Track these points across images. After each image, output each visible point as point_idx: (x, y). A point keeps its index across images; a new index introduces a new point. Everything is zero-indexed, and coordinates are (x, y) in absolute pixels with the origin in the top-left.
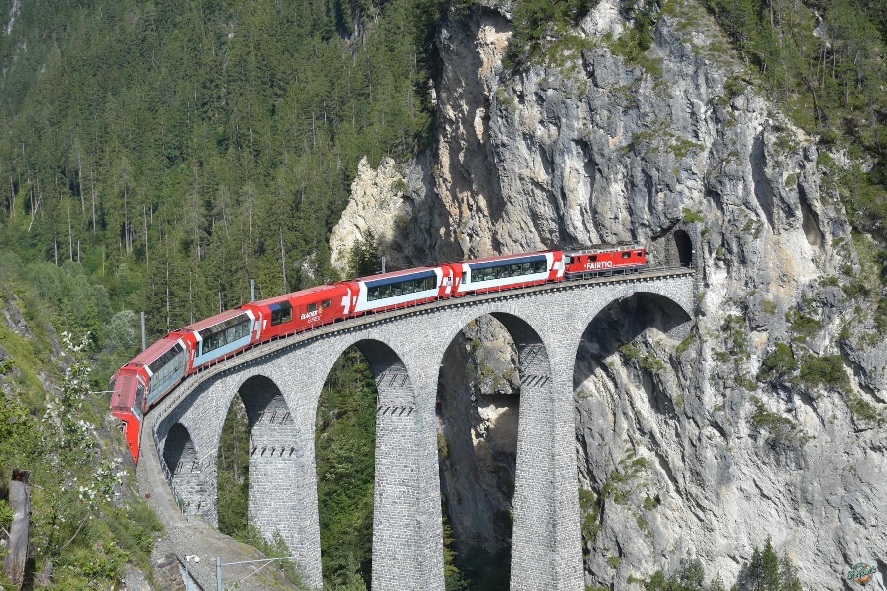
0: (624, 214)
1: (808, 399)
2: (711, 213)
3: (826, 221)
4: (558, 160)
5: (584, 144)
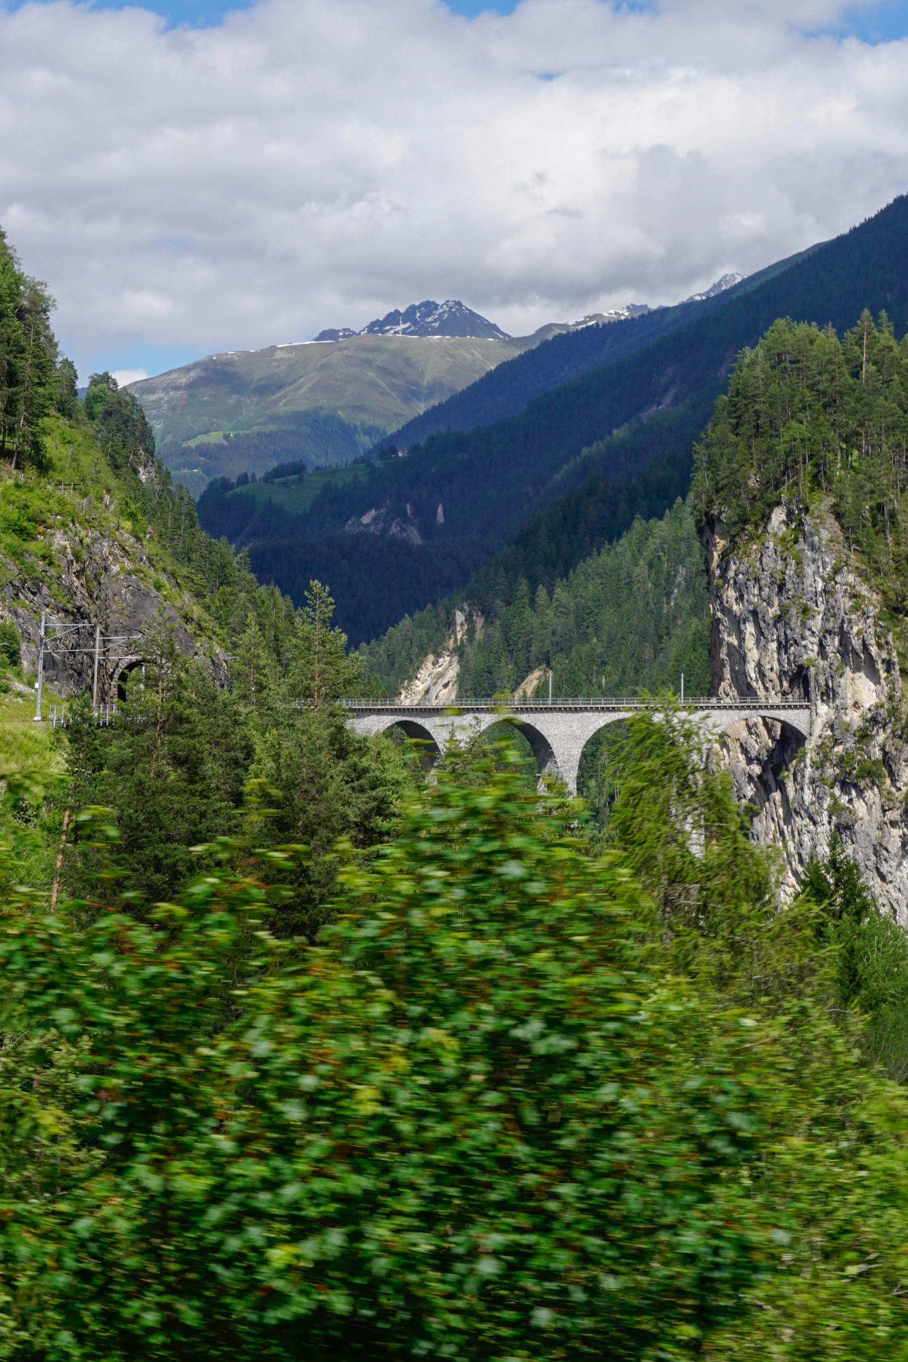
0: (776, 666)
1: (860, 793)
2: (821, 663)
3: (880, 661)
4: (742, 627)
5: (754, 613)
